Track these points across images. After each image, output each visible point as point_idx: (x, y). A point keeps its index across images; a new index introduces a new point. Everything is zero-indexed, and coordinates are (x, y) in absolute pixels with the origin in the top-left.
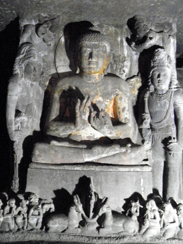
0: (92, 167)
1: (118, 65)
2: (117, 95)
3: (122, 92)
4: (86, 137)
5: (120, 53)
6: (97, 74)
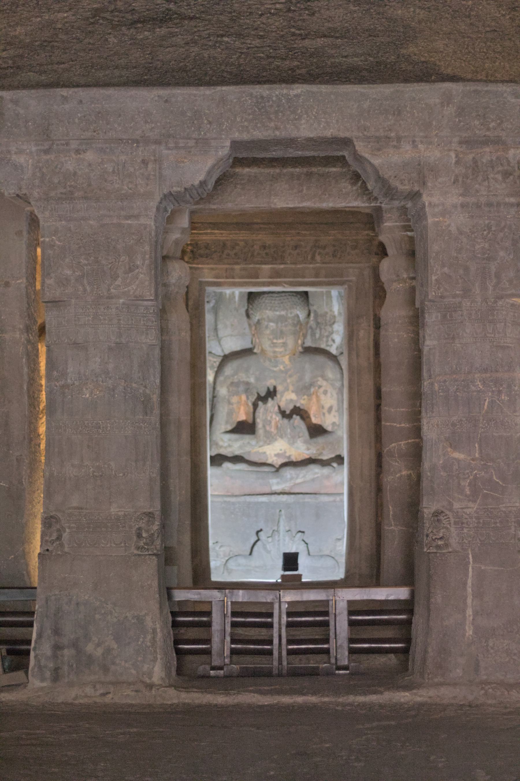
1: (323, 331)
2: (320, 387)
4: (273, 455)
5: (325, 309)
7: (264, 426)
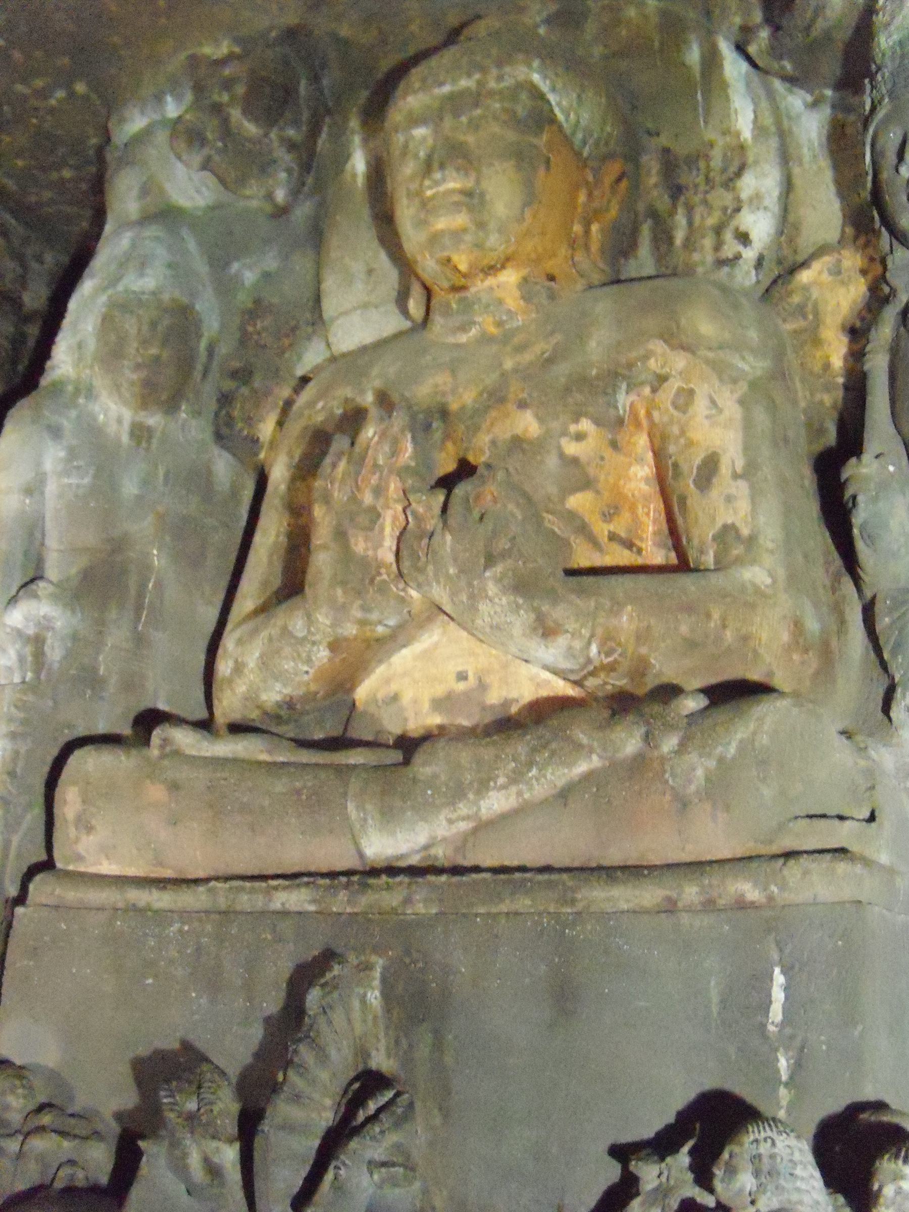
0: (389, 888)
1: (699, 211)
3: (693, 353)
4: (426, 706)
6: (510, 277)
7: (341, 535)
